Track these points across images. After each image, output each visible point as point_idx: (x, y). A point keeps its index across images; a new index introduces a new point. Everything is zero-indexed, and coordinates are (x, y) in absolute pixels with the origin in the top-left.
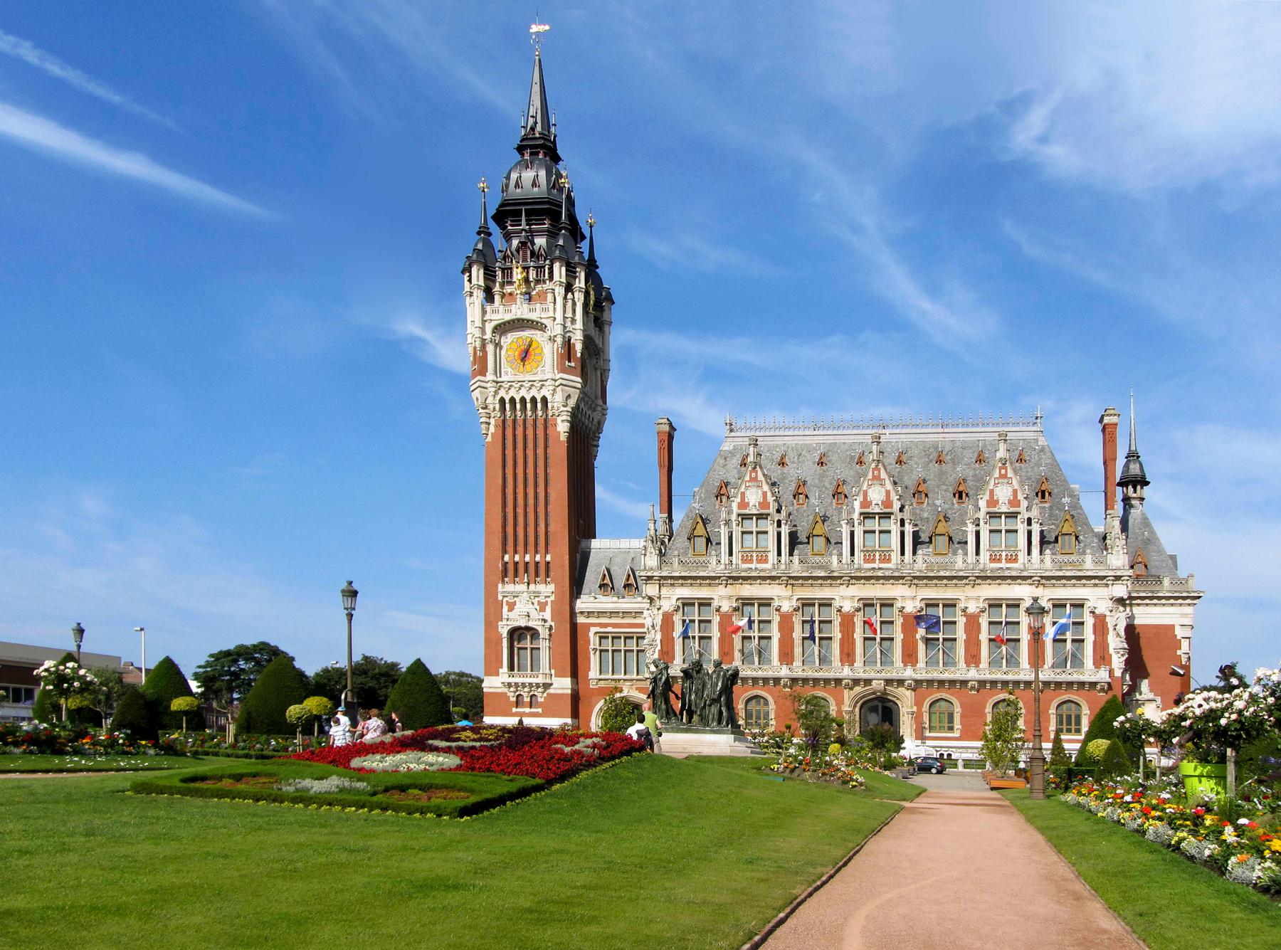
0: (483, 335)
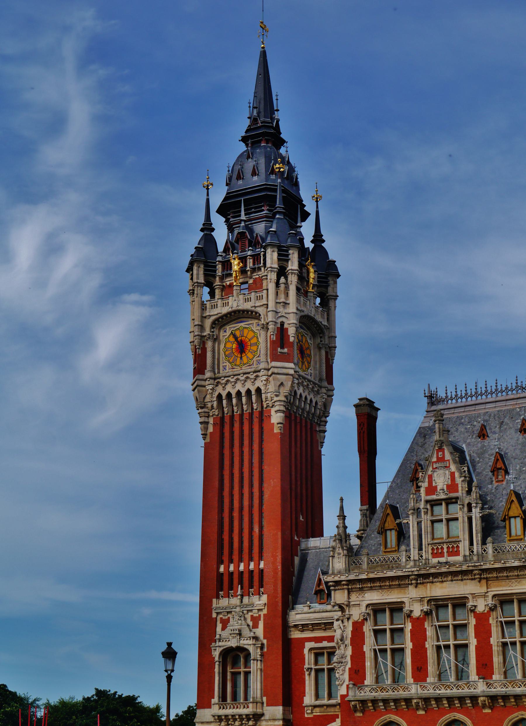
0: (201, 332)
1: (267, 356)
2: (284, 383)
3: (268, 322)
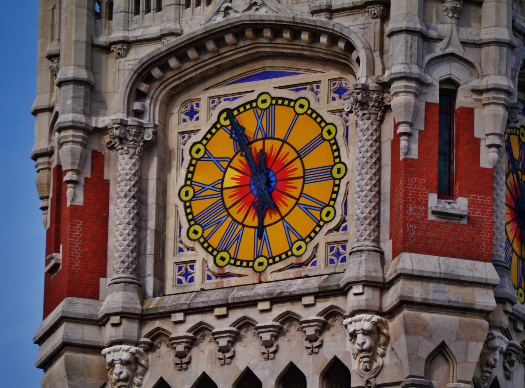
1: (378, 226)
2: (454, 347)
3: (386, 78)
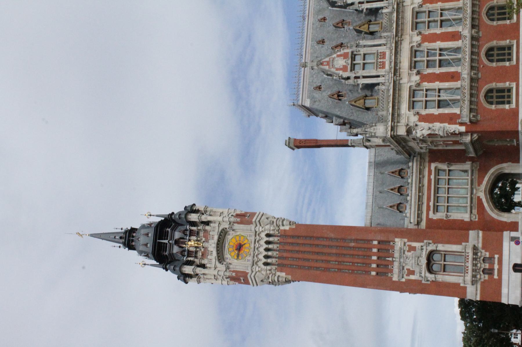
2: (267, 217)
